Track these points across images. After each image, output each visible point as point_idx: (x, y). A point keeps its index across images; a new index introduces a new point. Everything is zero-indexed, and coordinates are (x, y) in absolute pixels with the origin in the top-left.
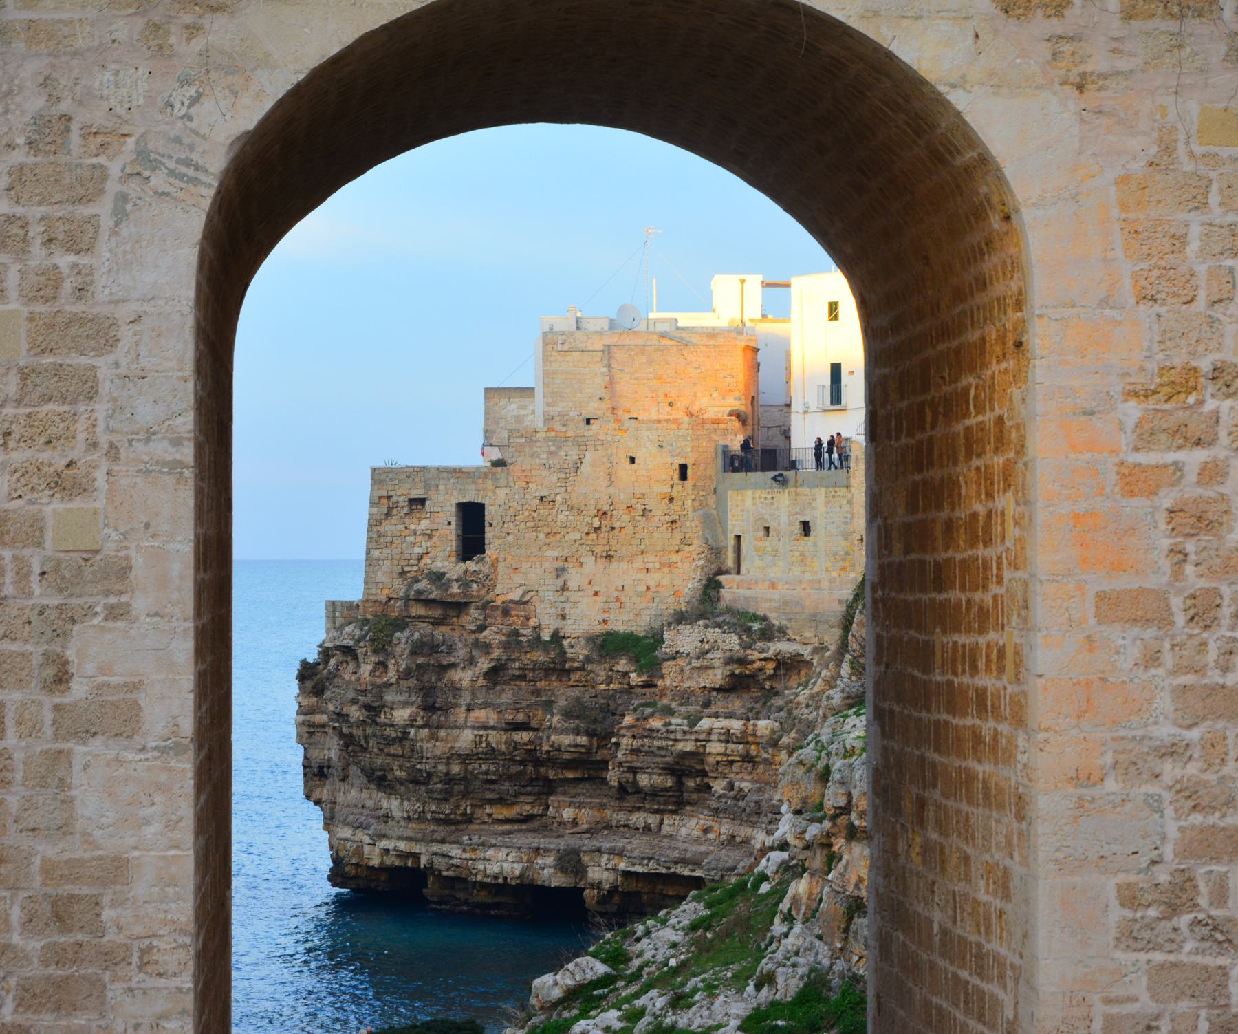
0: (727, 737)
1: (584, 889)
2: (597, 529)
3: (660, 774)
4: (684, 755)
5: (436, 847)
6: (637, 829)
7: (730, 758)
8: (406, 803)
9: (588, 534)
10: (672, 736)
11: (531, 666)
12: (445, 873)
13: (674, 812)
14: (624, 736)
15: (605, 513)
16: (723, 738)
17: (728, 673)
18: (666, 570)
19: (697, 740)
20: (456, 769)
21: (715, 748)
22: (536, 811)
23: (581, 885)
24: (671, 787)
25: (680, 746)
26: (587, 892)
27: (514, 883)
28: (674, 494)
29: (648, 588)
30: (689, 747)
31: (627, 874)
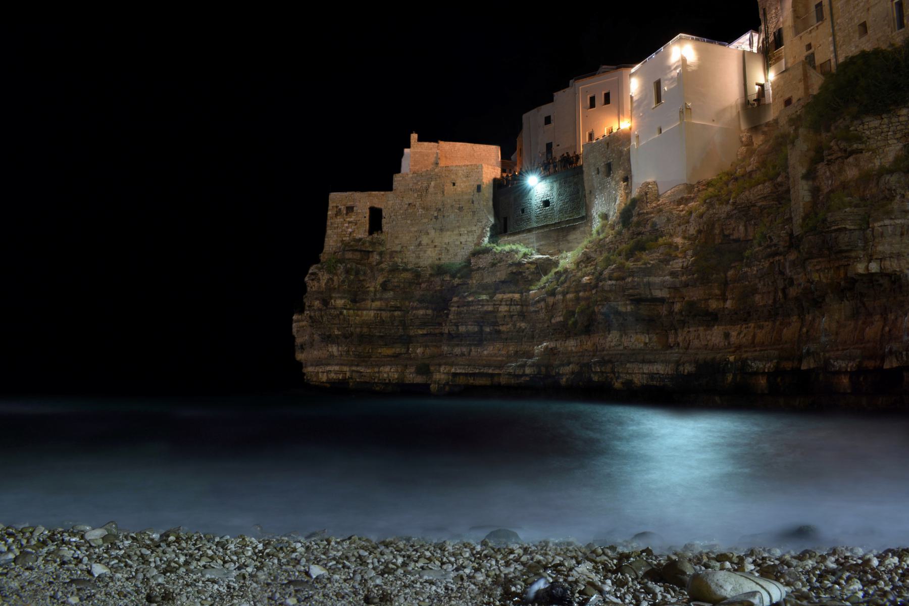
0: (512, 302)
1: (430, 384)
2: (436, 218)
3: (472, 325)
4: (487, 312)
5: (354, 368)
6: (457, 355)
7: (512, 314)
8: (340, 348)
9: (431, 220)
10: (481, 303)
11: (403, 281)
12: (358, 380)
13: (476, 345)
14: (453, 306)
15: (440, 210)
16: (508, 303)
17: (509, 272)
18: (470, 234)
19: (494, 305)
20: (365, 330)
21: (503, 309)
22: (403, 350)
23: (429, 382)
24: (477, 332)
25: (485, 308)
26: (431, 386)
27: (394, 382)
28: (474, 199)
29: (461, 243)
30: (490, 308)
31: (455, 375)
